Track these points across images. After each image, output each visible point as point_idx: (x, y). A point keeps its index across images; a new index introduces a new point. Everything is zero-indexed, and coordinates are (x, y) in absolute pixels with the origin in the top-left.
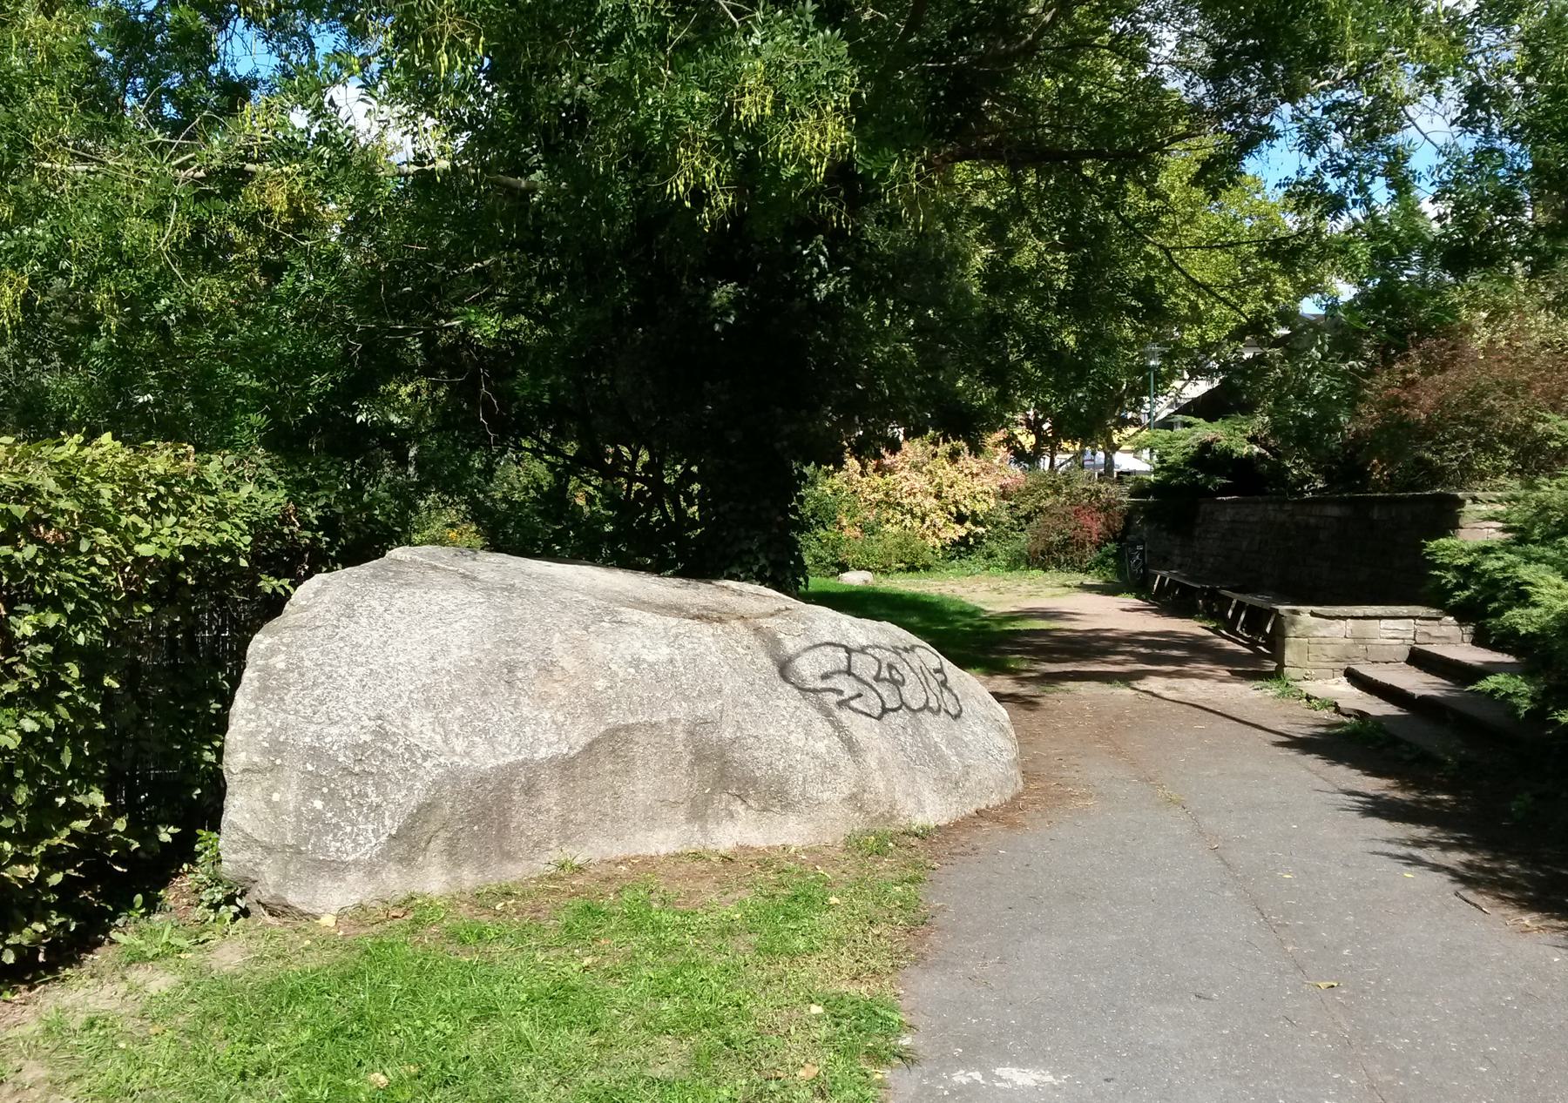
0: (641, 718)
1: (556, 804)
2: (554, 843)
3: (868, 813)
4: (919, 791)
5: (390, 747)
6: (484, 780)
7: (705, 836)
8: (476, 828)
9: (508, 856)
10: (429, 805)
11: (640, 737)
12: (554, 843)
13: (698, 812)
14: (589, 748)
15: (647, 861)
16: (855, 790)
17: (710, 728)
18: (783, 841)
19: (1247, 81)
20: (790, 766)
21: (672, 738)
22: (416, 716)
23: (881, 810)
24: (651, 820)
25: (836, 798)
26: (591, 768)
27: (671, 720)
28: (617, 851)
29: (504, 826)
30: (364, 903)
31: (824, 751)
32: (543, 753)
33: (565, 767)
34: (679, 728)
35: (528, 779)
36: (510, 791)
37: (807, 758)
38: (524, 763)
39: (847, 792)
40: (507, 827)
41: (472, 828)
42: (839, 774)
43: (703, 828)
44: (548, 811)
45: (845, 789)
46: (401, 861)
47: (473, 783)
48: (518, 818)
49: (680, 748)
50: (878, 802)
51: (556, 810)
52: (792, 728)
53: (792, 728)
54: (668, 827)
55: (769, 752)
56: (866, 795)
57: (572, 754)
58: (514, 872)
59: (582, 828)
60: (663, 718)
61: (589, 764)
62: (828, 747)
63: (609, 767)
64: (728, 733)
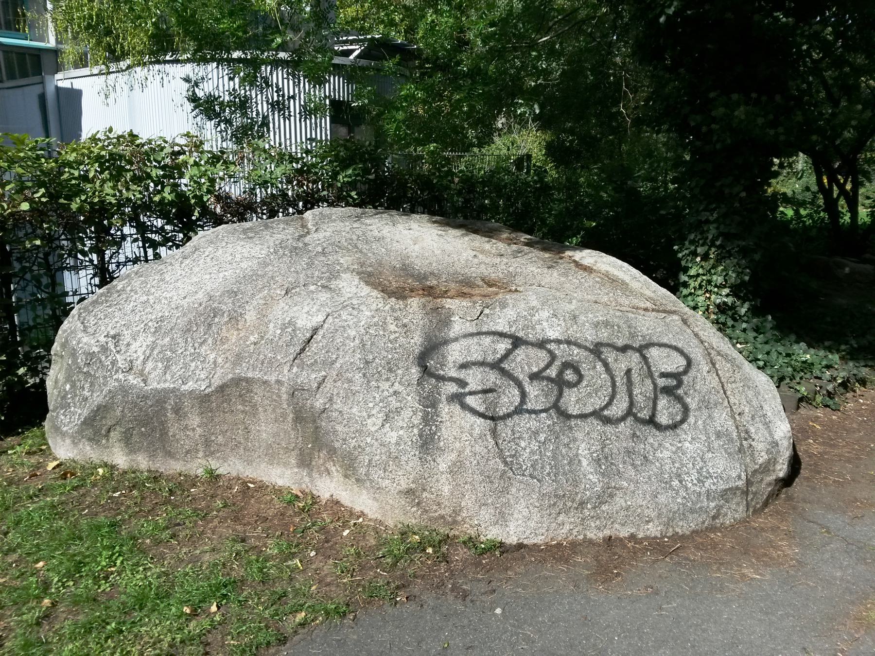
0: (257, 375)
1: (198, 426)
2: (201, 454)
3: (427, 511)
4: (508, 504)
5: (103, 359)
6: (145, 397)
7: (312, 481)
8: (143, 429)
9: (170, 454)
10: (105, 406)
11: (256, 388)
12: (201, 454)
13: (305, 462)
14: (222, 388)
15: (261, 487)
16: (413, 486)
17: (306, 395)
18: (362, 508)
19: (174, 30)
20: (359, 446)
21: (280, 397)
22: (141, 339)
23: (442, 512)
24: (272, 456)
25: (394, 489)
26: (225, 405)
27: (278, 382)
28: (249, 472)
29: (164, 433)
30: (75, 459)
31: (393, 441)
32: (190, 386)
33: (203, 400)
34: (284, 389)
35: (176, 403)
36: (165, 409)
37: (376, 443)
38: (173, 390)
39: (404, 486)
40: (166, 433)
41: (140, 429)
42: (399, 466)
43: (310, 475)
44: (194, 430)
45: (402, 482)
46: (90, 440)
47: (138, 397)
48: (173, 429)
49: (285, 406)
50: (439, 504)
51: (199, 431)
52: (374, 412)
53: (374, 412)
54: (285, 466)
55: (346, 429)
56: (425, 495)
57: (209, 390)
58: (173, 467)
59: (222, 448)
60: (272, 378)
61: (223, 402)
62: (400, 438)
63: (240, 407)
64: (319, 403)
